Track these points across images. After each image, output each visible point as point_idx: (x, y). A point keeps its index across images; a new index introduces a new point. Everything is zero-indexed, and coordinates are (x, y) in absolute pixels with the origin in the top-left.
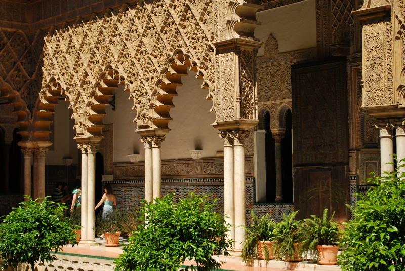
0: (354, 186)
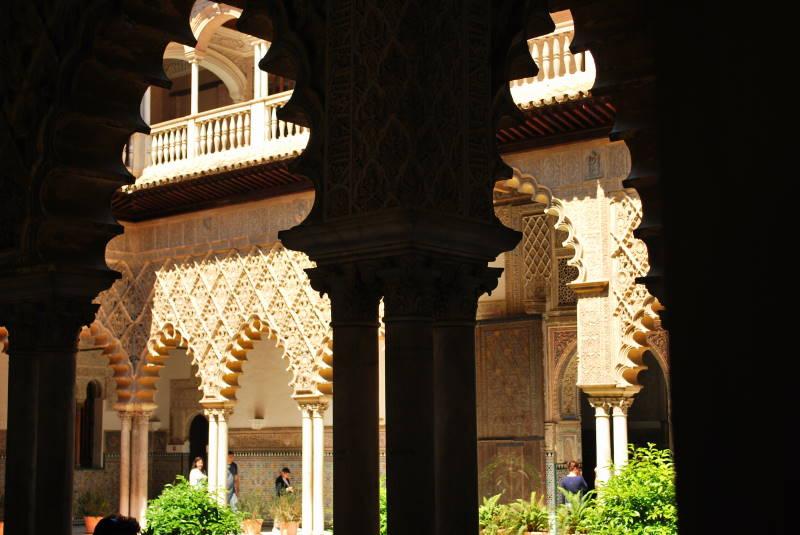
0: (550, 464)
